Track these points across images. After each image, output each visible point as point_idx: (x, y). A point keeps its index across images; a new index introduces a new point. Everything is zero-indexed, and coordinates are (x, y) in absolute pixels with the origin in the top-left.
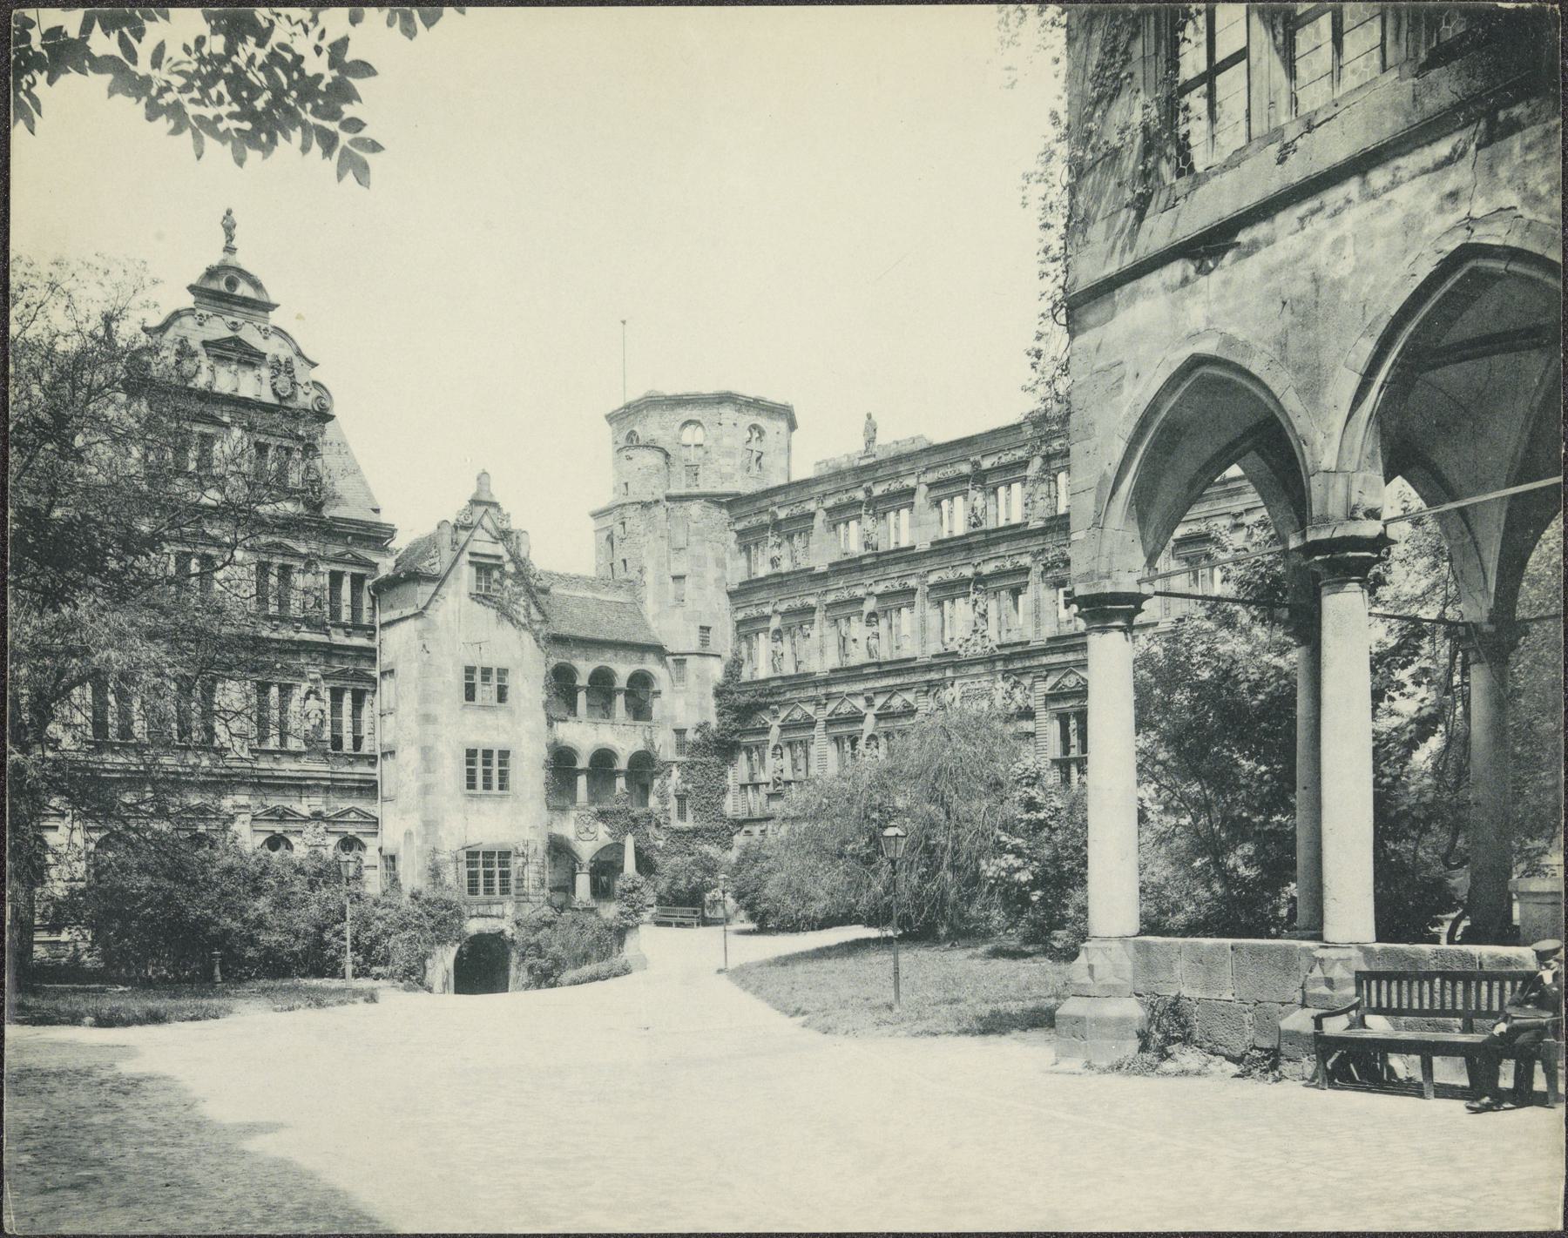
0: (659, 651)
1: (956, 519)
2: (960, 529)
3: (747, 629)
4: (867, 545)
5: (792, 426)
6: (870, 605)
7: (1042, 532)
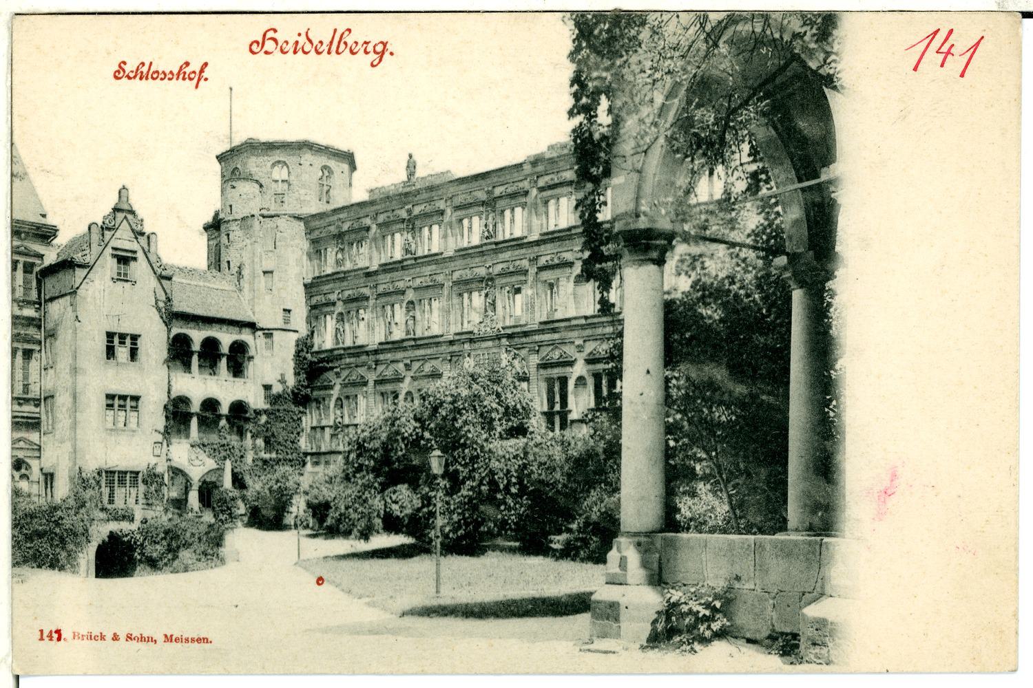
0: (252, 326)
1: (474, 232)
2: (476, 240)
3: (317, 311)
4: (407, 251)
5: (353, 167)
6: (410, 295)
7: (537, 243)
